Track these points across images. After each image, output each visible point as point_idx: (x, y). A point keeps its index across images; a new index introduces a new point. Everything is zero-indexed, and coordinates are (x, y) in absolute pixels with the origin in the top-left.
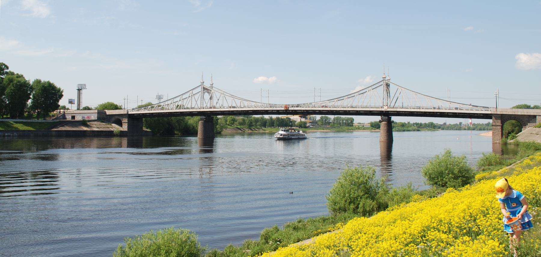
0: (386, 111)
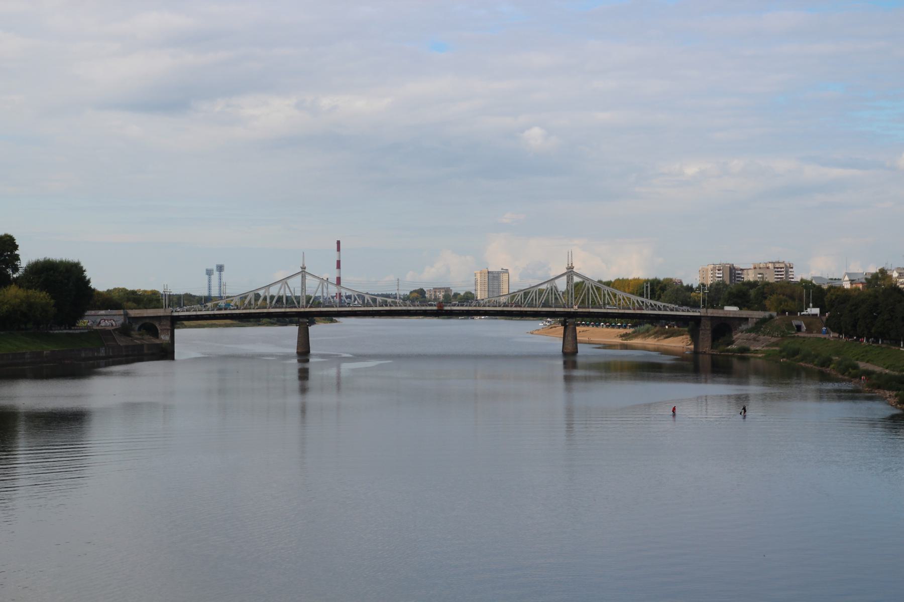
0: (574, 312)
